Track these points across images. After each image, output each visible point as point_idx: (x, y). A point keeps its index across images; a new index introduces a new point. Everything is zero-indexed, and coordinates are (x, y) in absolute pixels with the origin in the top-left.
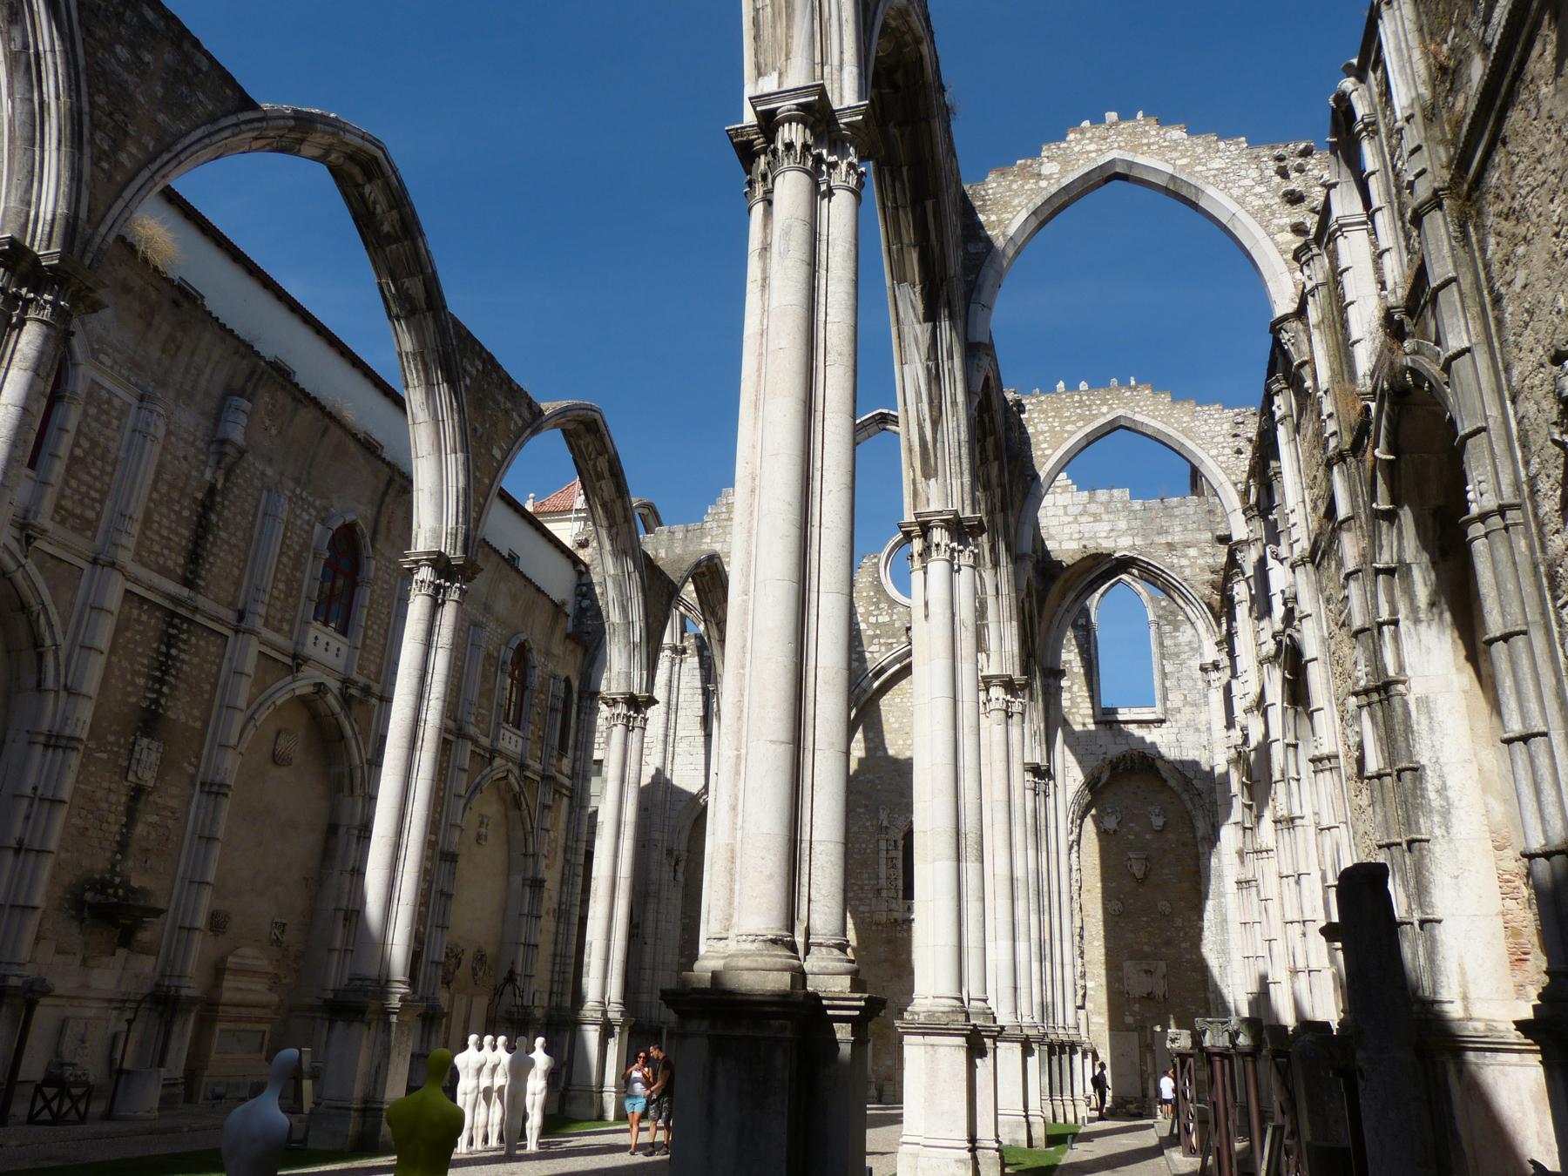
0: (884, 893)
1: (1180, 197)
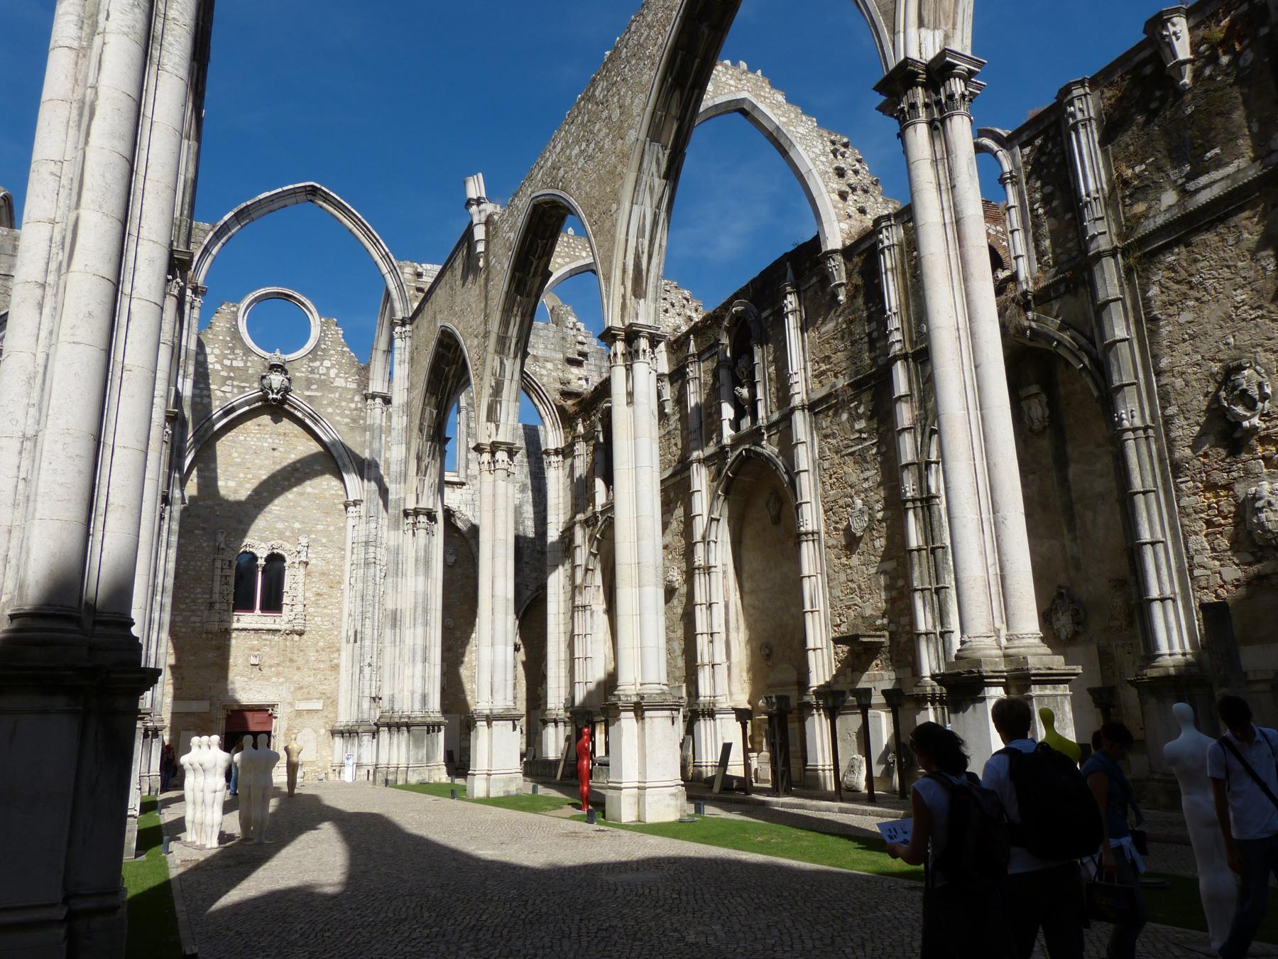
0: (217, 606)
1: (778, 143)
